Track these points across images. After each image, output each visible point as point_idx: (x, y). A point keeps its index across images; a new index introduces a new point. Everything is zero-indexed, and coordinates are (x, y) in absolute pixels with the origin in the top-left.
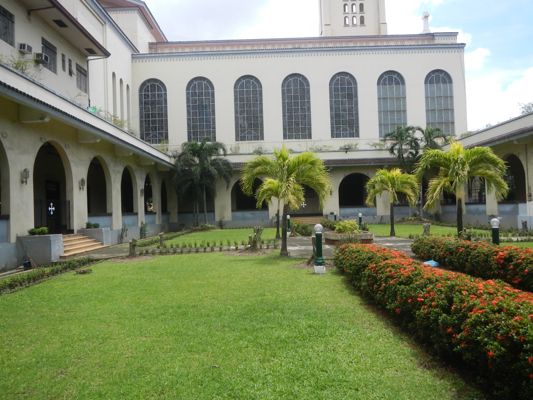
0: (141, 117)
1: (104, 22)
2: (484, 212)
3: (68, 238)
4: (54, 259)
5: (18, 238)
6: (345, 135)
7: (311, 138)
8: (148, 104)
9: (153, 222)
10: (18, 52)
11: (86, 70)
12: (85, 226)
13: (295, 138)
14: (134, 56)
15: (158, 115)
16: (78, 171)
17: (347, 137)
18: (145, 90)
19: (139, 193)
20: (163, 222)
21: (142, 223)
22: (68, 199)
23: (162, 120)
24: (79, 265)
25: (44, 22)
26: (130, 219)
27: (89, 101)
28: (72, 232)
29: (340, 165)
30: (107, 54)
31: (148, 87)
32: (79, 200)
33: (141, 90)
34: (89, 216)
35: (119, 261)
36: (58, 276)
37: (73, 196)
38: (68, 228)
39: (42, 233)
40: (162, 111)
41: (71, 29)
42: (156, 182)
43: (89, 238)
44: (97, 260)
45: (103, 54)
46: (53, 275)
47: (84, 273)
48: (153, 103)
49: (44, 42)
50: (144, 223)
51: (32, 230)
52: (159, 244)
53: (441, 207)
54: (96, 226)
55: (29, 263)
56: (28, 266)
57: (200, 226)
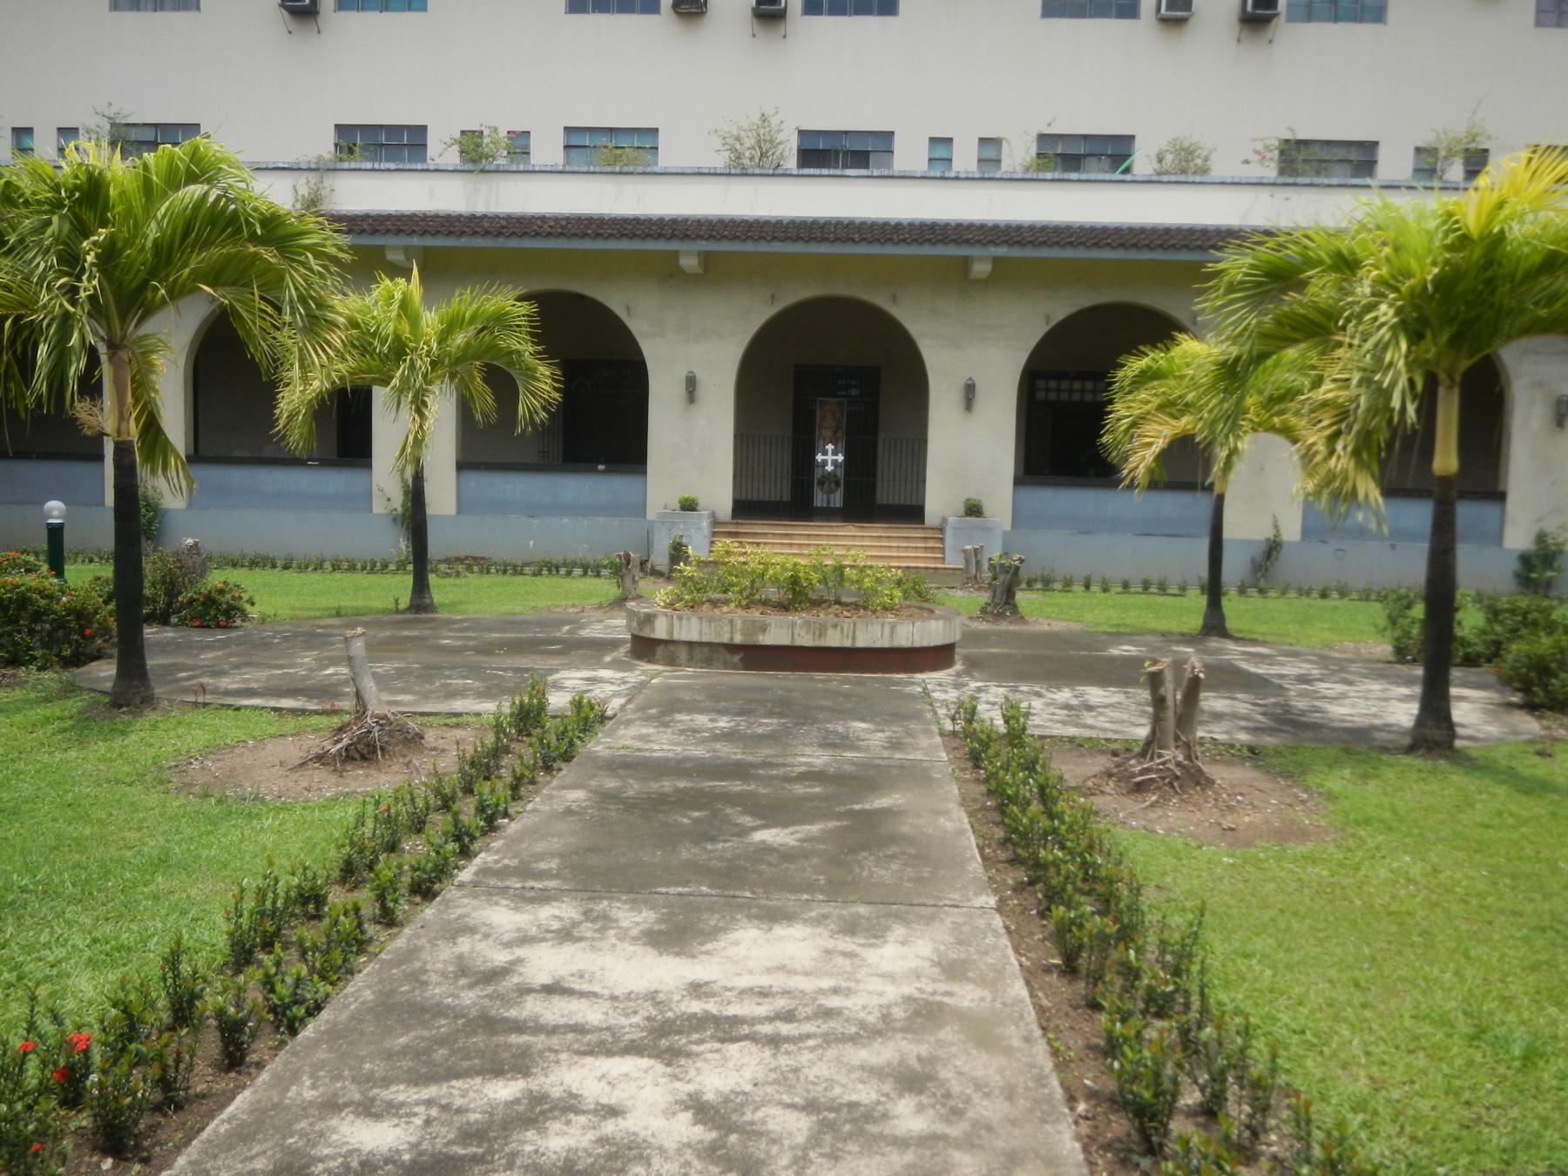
10: (1154, 22)
21: (1541, 538)
34: (1018, 482)
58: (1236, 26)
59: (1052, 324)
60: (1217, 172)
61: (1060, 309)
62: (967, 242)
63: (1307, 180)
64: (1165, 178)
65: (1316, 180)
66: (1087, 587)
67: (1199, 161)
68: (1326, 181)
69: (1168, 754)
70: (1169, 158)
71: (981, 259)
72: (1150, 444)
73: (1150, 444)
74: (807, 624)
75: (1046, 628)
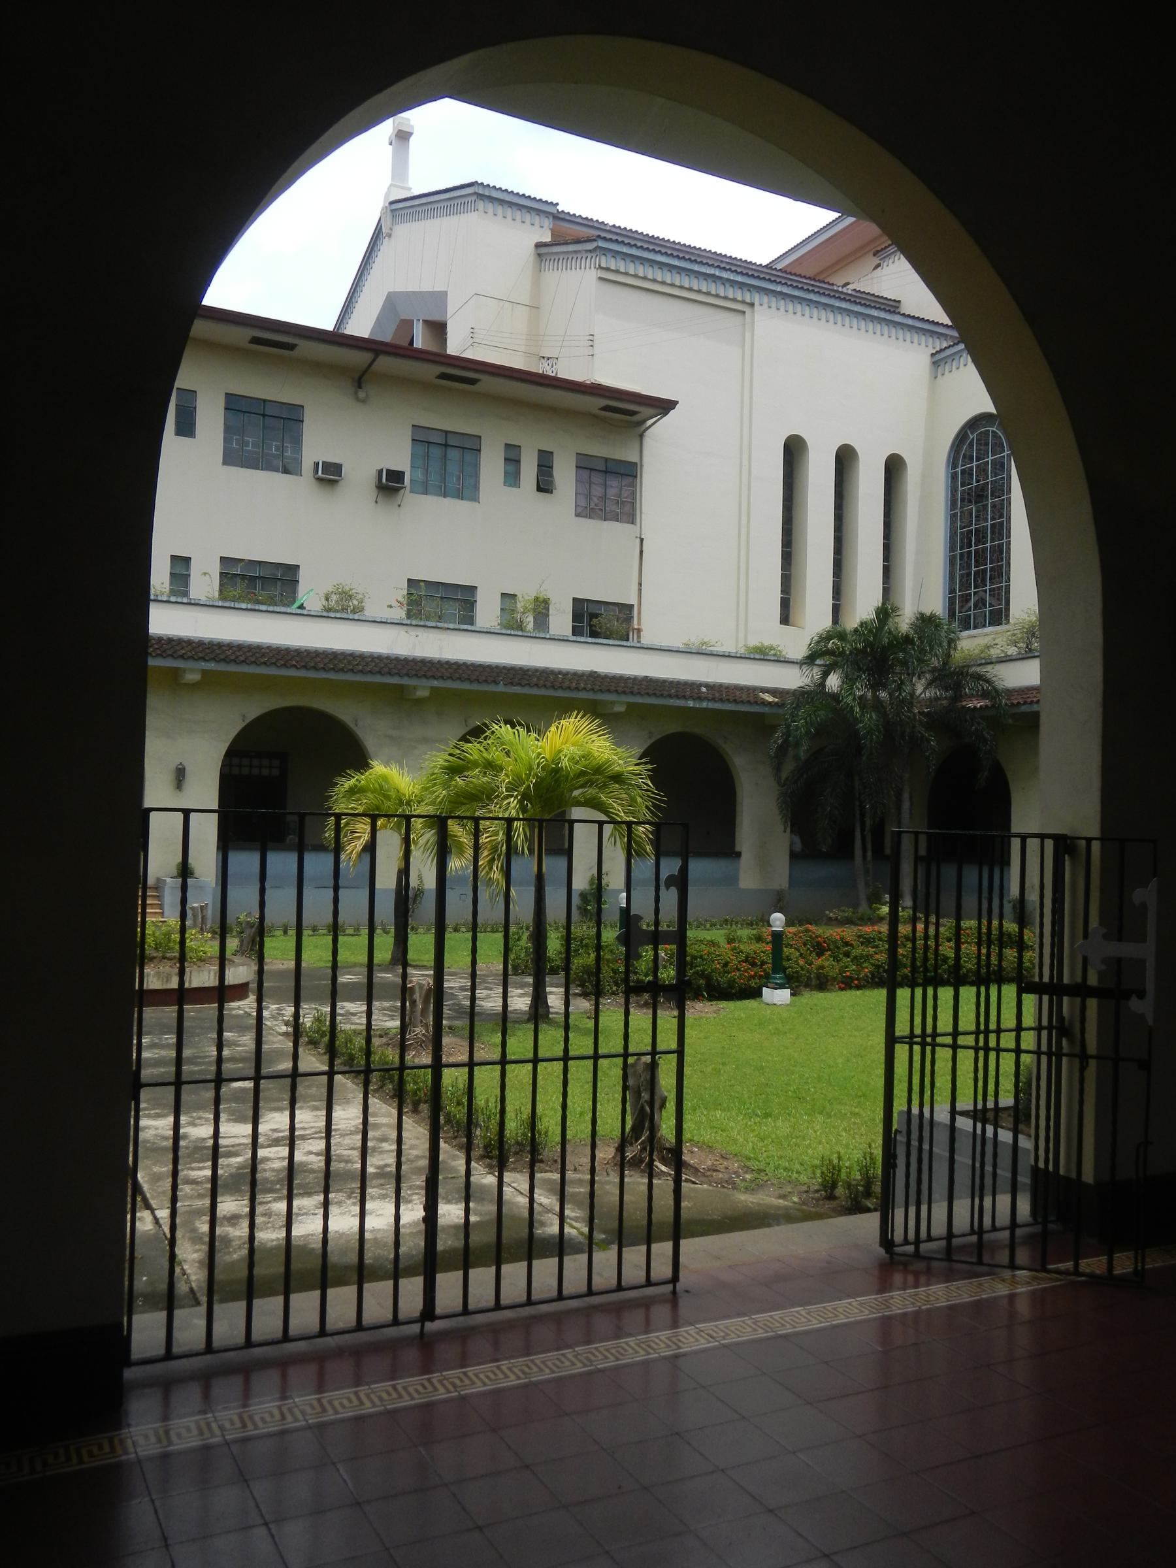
0: (952, 548)
1: (743, 302)
8: (970, 501)
9: (732, 880)
11: (633, 457)
14: (938, 357)
15: (993, 533)
18: (964, 456)
20: (792, 881)
23: (1000, 546)
25: (424, 387)
27: (642, 540)
30: (665, 406)
31: (971, 445)
33: (953, 461)
40: (1001, 516)
41: (487, 383)
45: (651, 411)
48: (980, 496)
49: (422, 440)
57: (863, 908)
58: (374, 492)
59: (248, 721)
60: (370, 612)
61: (254, 710)
62: (182, 657)
63: (433, 624)
64: (332, 615)
65: (439, 624)
66: (285, 932)
67: (356, 602)
68: (446, 626)
69: (418, 1030)
70: (334, 597)
71: (192, 671)
72: (360, 837)
73: (360, 837)
74: (158, 974)
75: (284, 967)
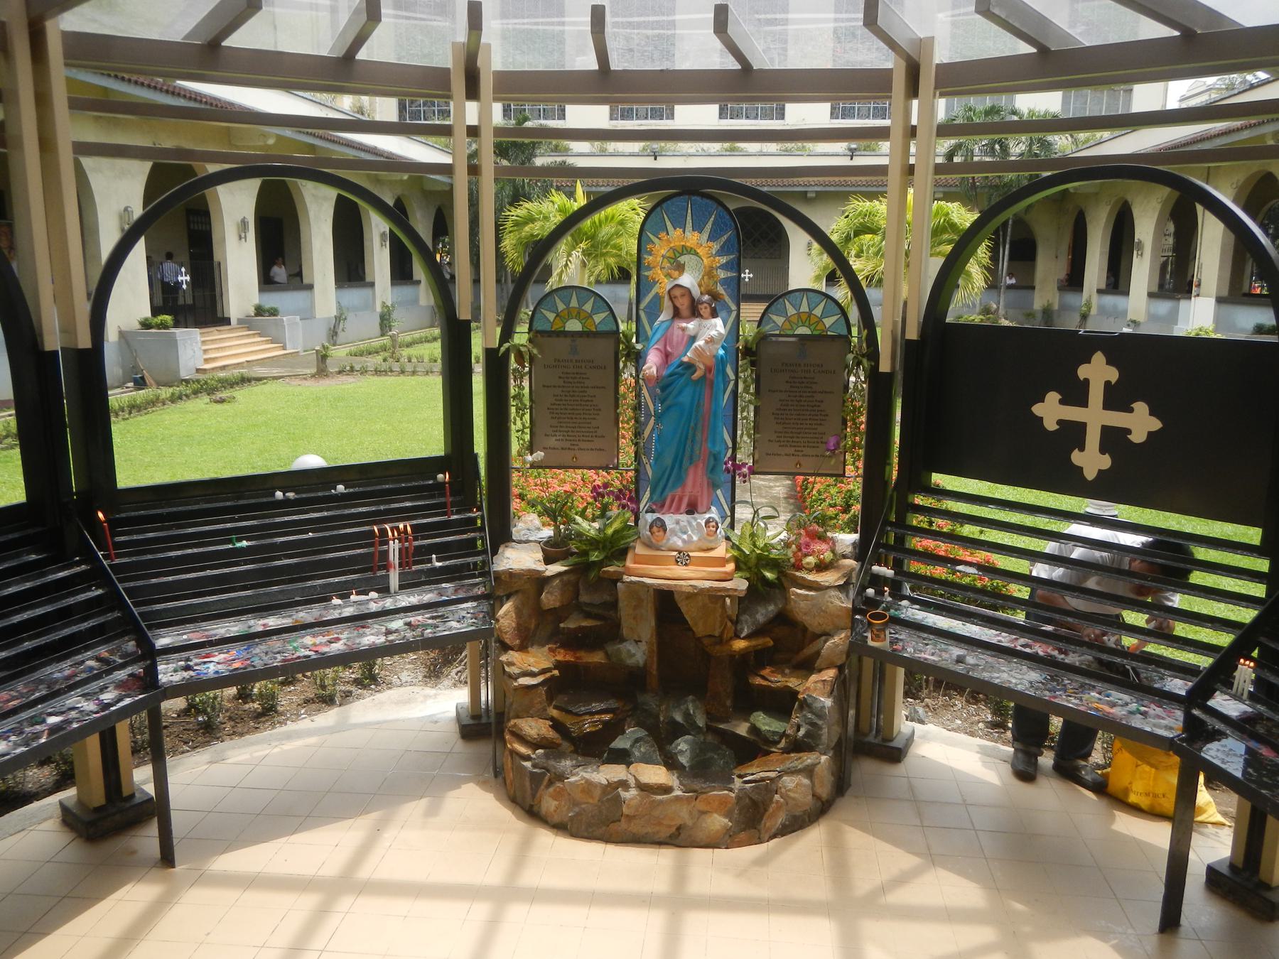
2: (1125, 313)
3: (214, 333)
4: (184, 374)
5: (122, 334)
6: (864, 112)
7: (783, 118)
9: (415, 301)
12: (252, 312)
13: (747, 117)
16: (236, 206)
17: (868, 117)
19: (376, 240)
22: (217, 257)
24: (214, 387)
26: (354, 296)
28: (227, 321)
29: (832, 189)
32: (239, 260)
34: (261, 290)
35: (297, 382)
36: (181, 405)
37: (225, 252)
38: (219, 315)
39: (163, 326)
42: (418, 215)
43: (260, 335)
44: (259, 379)
46: (173, 402)
47: (222, 401)
50: (389, 303)
51: (146, 319)
52: (387, 354)
53: (1057, 295)
54: (273, 312)
55: (142, 378)
56: (140, 383)
